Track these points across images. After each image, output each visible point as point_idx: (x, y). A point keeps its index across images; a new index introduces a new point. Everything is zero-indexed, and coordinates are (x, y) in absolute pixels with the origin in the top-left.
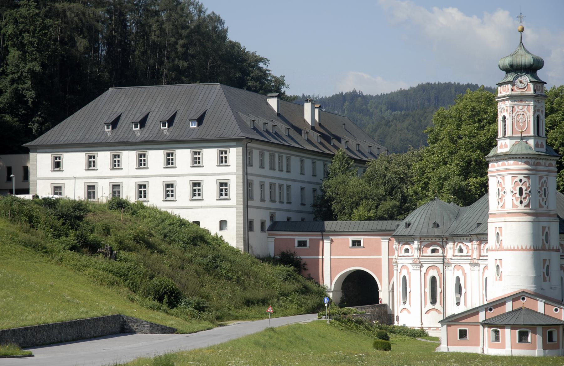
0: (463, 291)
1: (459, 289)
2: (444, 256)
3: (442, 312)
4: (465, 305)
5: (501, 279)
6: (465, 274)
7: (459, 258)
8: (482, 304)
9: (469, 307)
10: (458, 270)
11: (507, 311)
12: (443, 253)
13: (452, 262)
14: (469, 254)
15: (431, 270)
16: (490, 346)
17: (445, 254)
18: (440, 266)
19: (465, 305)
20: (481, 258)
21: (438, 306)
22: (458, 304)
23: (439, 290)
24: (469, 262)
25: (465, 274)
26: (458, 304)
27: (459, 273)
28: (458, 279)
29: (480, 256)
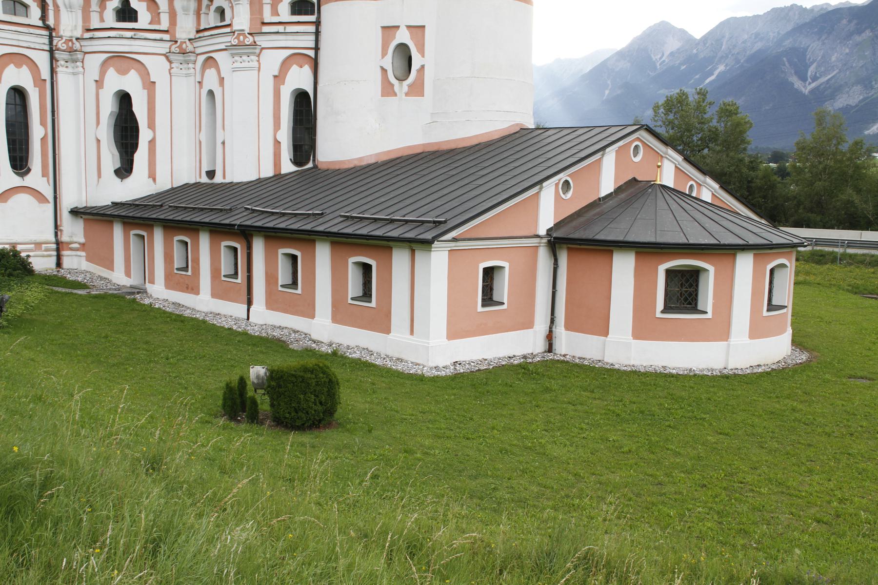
0: (144, 135)
1: (126, 131)
2: (47, 27)
3: (51, 198)
4: (152, 176)
5: (417, 89)
6: (150, 86)
7: (129, 34)
8: (268, 172)
9: (164, 183)
10: (123, 72)
11: (603, 193)
12: (44, 18)
13: (89, 46)
14: (165, 24)
15: (12, 66)
16: (644, 328)
17: (51, 22)
18: (42, 60)
19: (152, 176)
20: (266, 29)
21: (36, 178)
22: (125, 170)
23: (37, 132)
24: (164, 48)
25: (150, 86)
26: (125, 170)
27: (132, 83)
28: (124, 99)
29: (264, 24)
